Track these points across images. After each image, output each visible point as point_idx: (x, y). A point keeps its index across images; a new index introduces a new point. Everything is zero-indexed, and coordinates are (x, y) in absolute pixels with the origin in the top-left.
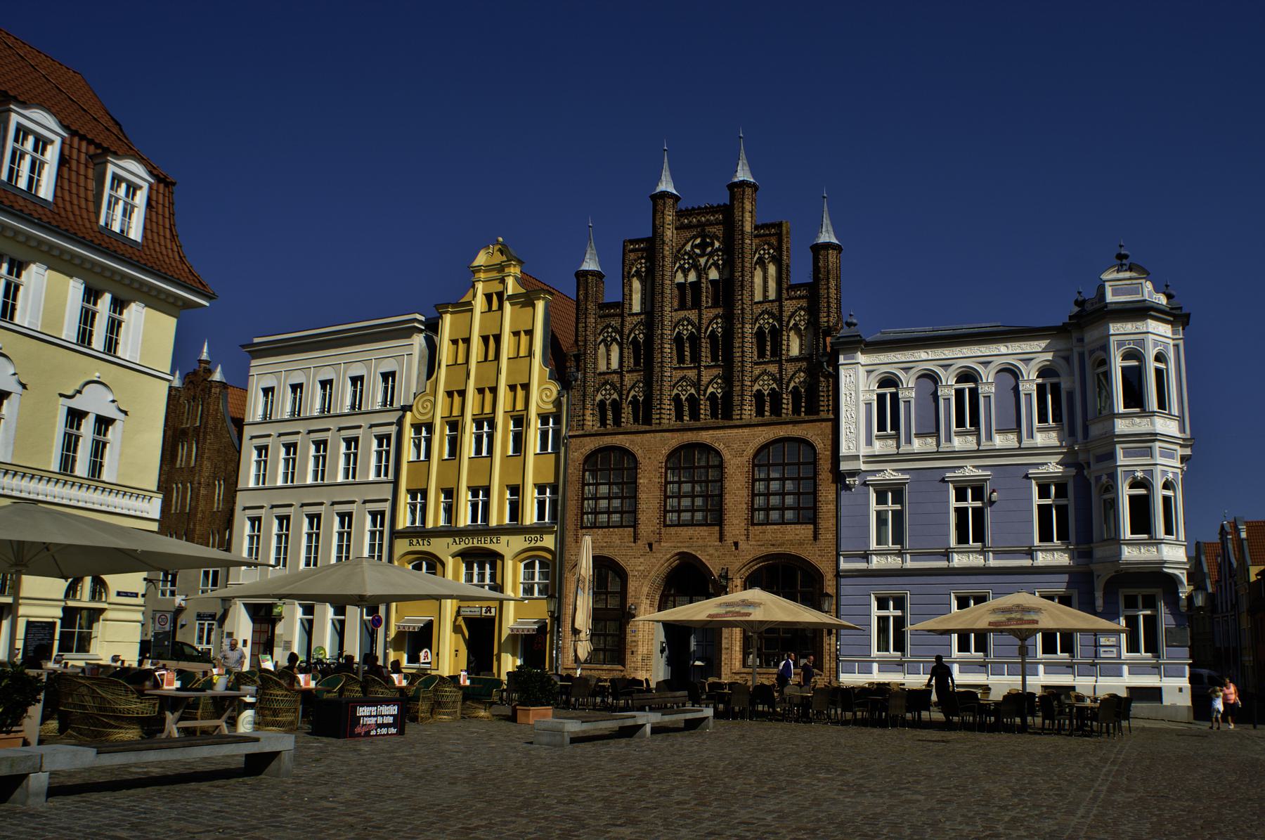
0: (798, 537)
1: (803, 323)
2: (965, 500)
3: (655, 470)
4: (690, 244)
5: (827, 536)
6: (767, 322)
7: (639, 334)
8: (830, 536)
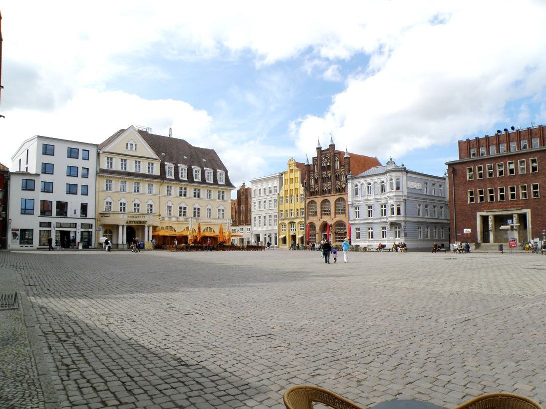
6: (338, 174)
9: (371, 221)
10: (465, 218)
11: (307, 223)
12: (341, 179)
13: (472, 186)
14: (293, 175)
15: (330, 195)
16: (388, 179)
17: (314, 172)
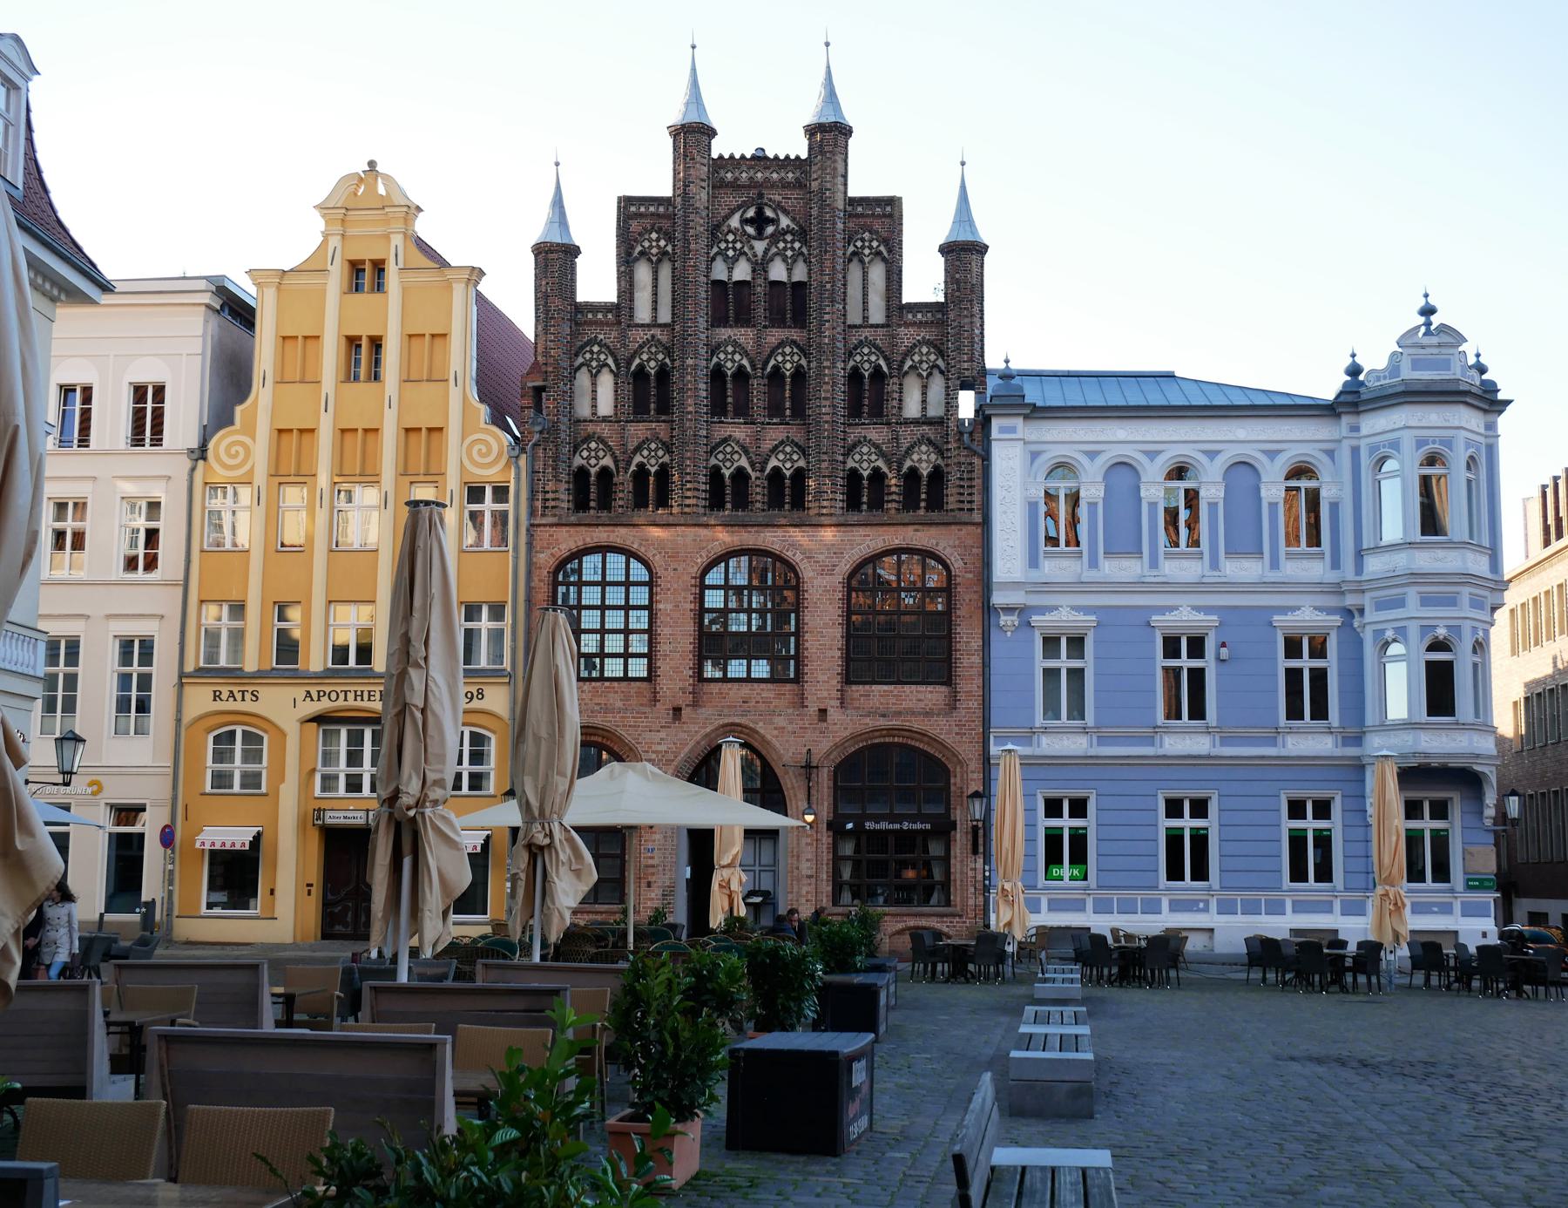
0: (922, 705)
1: (925, 366)
2: (1177, 655)
3: (685, 590)
4: (737, 216)
5: (970, 704)
6: (867, 361)
7: (649, 360)
8: (974, 704)
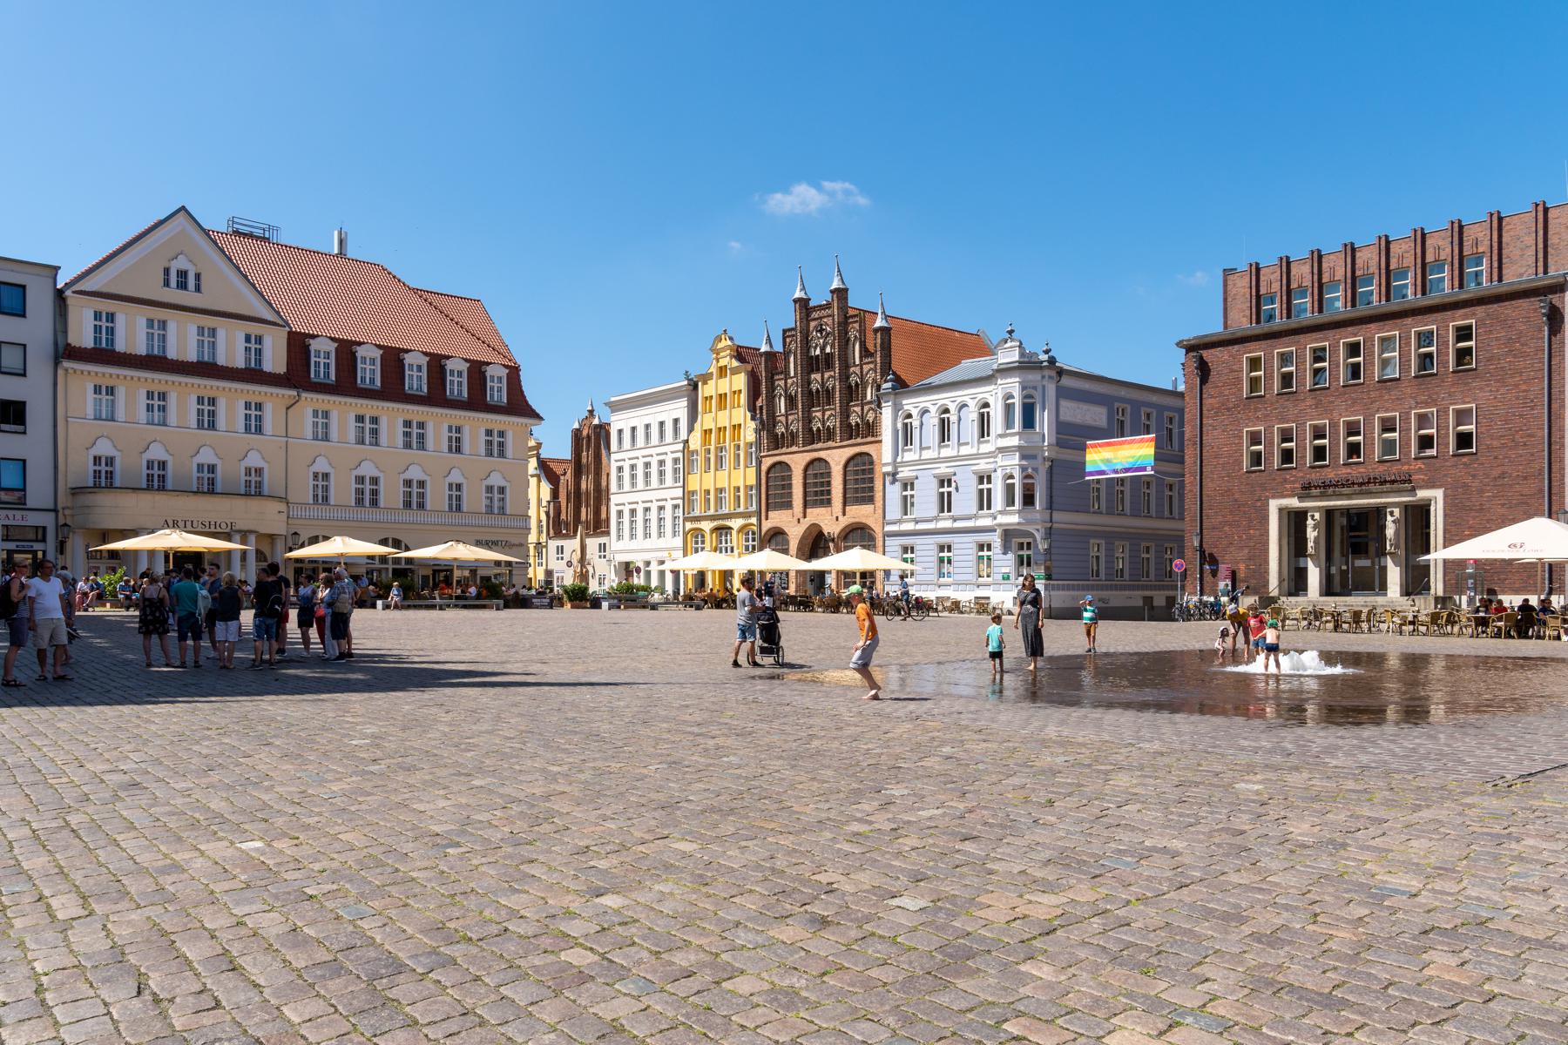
8: (881, 511)
9: (947, 524)
10: (1229, 518)
11: (764, 529)
12: (864, 395)
13: (1259, 414)
14: (724, 385)
15: (830, 444)
16: (1000, 396)
17: (787, 376)
